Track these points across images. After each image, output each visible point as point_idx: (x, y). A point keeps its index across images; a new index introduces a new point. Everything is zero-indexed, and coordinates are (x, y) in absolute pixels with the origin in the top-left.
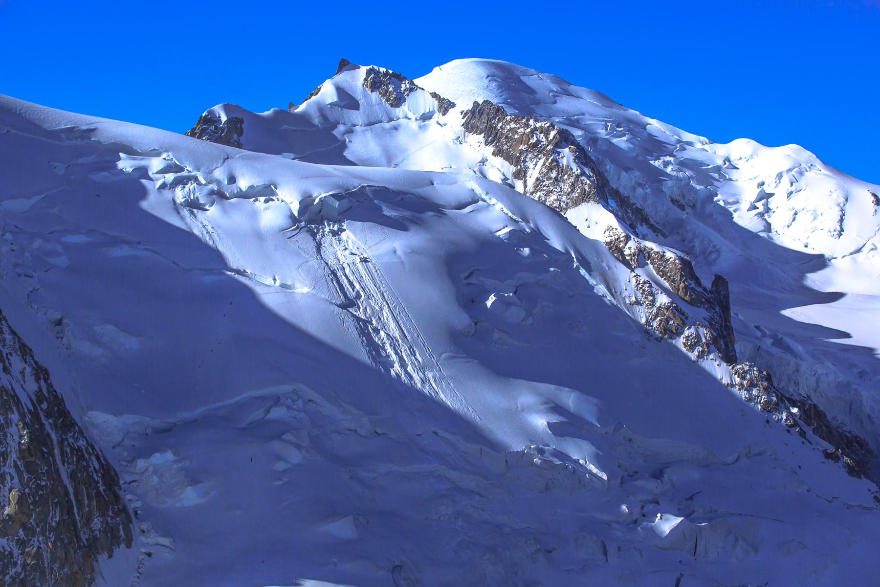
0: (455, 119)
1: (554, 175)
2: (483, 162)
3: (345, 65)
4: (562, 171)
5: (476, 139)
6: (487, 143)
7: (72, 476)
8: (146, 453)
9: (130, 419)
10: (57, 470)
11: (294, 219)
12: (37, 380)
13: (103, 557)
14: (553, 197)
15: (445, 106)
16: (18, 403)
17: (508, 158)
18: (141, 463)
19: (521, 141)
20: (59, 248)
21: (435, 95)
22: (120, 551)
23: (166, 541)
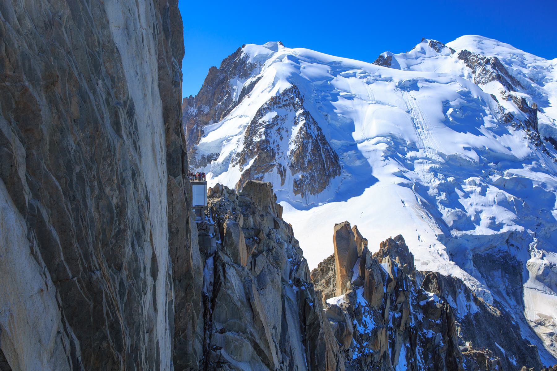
0: (456, 55)
1: (484, 72)
2: (463, 69)
3: (423, 40)
4: (487, 71)
5: (462, 61)
6: (465, 63)
7: (325, 157)
8: (347, 151)
9: (343, 142)
10: (321, 155)
11: (396, 87)
12: (318, 131)
13: (332, 178)
14: (484, 79)
15: (453, 51)
16: (312, 137)
17: (471, 67)
18: (345, 154)
19: (475, 62)
20: (329, 95)
21: (450, 48)
22: (337, 177)
23: (349, 175)
